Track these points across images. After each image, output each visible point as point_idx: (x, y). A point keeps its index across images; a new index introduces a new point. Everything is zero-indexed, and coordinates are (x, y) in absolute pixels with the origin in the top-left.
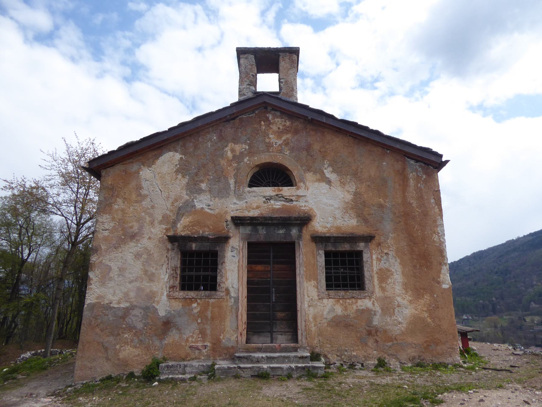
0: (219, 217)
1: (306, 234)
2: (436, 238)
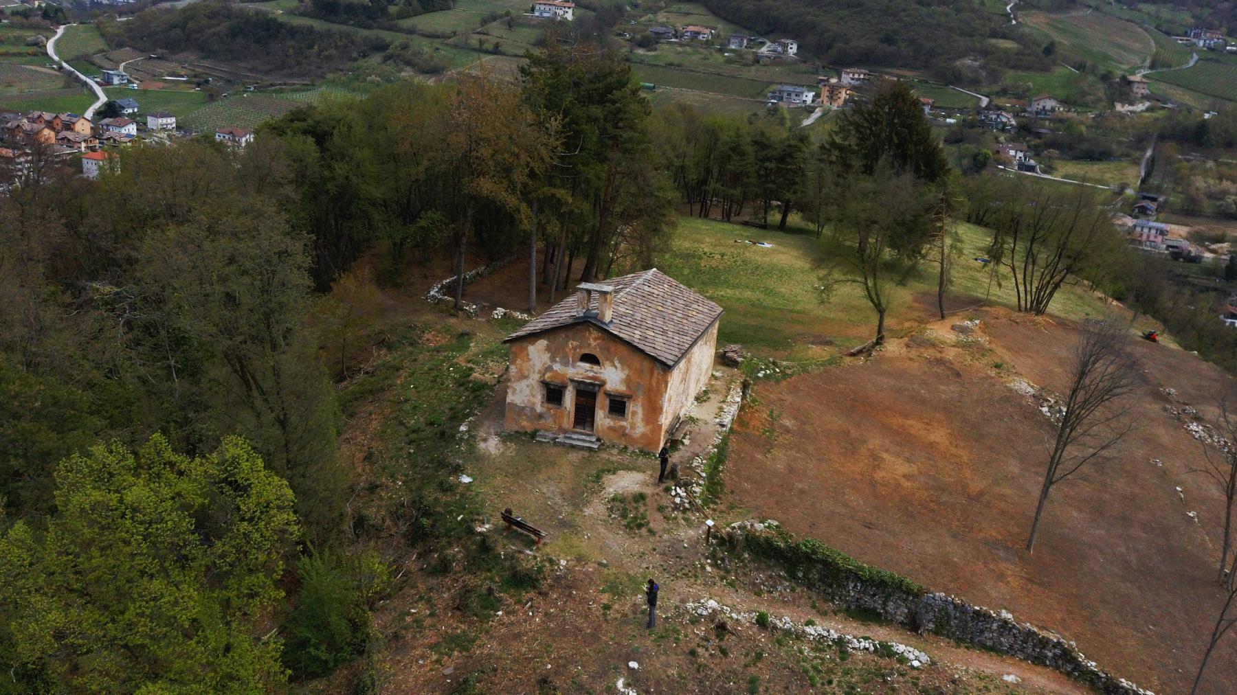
0: (564, 376)
1: (602, 391)
2: (660, 402)
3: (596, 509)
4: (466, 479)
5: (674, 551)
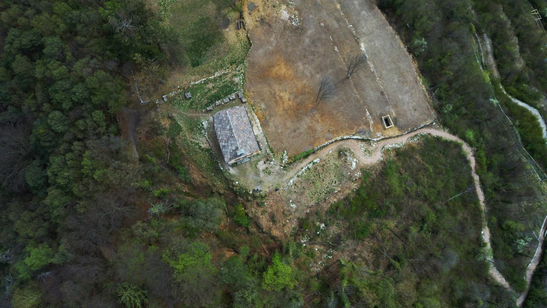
3: (262, 175)
4: (237, 183)
5: (278, 173)
